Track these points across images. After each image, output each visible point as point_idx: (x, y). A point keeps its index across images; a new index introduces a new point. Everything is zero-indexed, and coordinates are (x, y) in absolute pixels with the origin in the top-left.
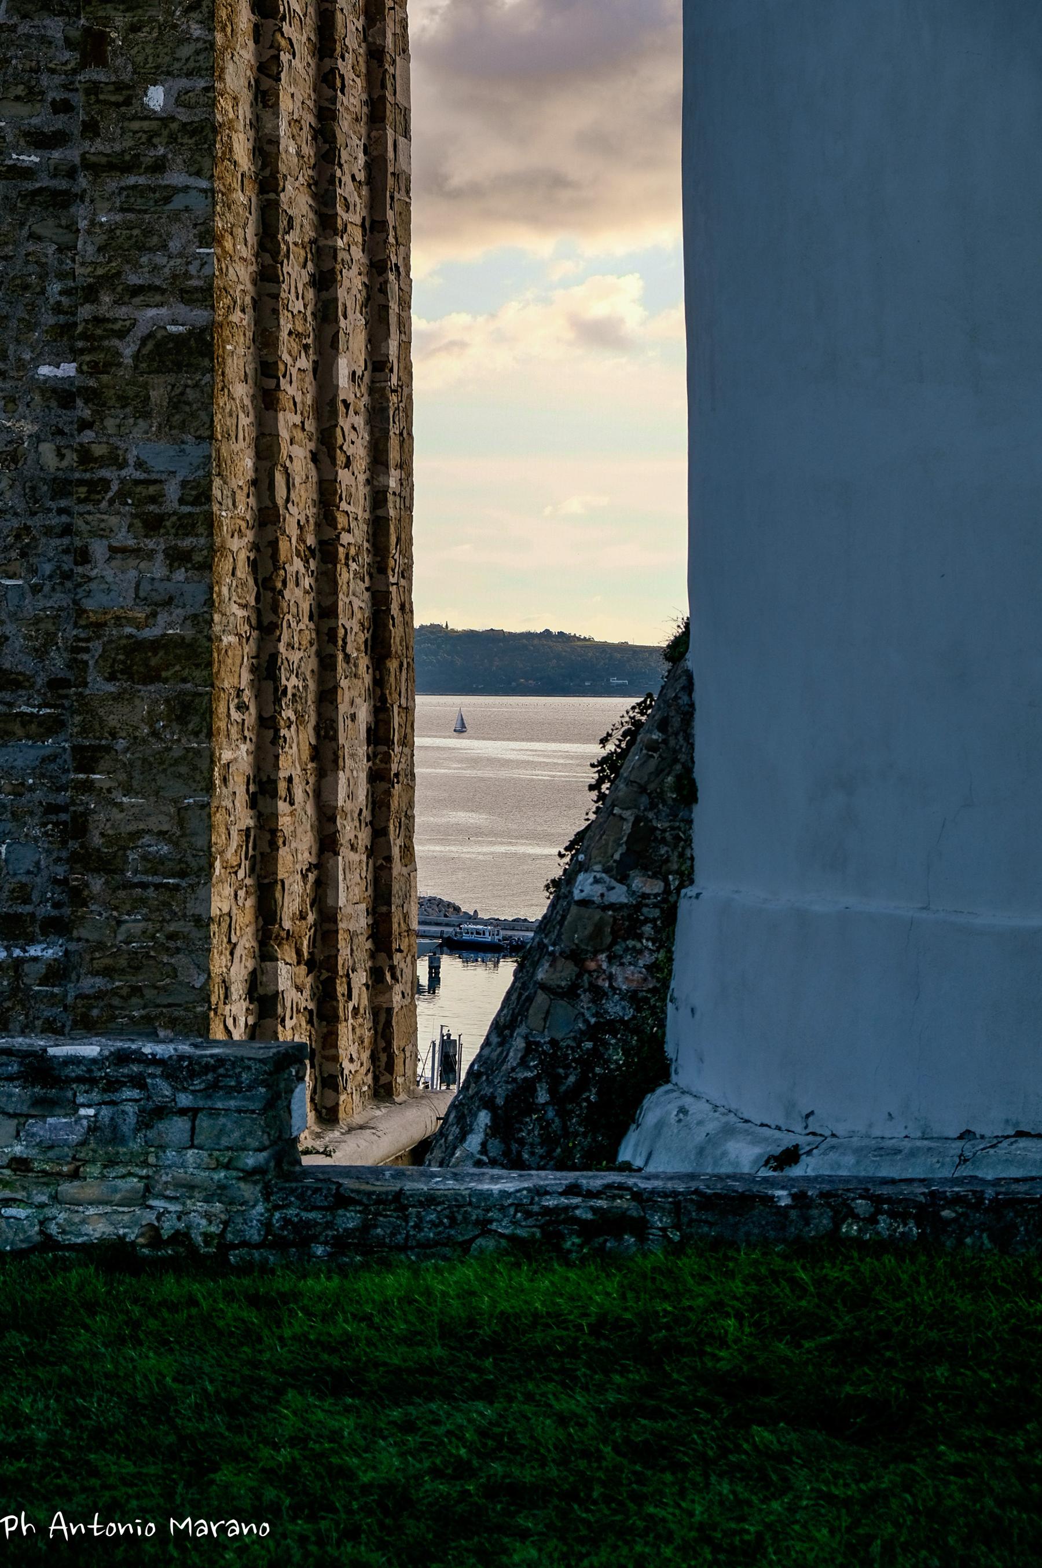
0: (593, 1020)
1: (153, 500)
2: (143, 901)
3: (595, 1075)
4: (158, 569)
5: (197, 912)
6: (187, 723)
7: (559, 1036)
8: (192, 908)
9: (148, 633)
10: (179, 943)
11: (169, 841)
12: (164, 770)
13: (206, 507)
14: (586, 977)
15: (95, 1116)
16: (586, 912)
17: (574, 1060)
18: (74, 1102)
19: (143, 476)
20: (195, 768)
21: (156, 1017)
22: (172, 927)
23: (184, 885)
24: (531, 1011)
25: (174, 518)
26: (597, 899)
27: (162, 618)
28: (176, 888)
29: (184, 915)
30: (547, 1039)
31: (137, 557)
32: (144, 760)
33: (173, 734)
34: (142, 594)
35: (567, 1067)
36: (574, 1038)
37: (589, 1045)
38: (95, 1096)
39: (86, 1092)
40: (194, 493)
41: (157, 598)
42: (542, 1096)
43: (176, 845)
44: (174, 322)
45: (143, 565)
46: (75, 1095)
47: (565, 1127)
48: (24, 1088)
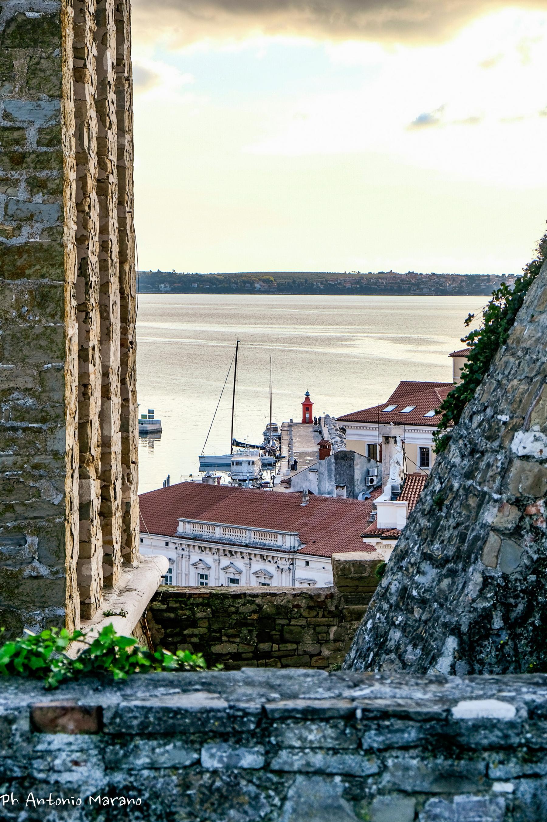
0: (535, 557)
1: (17, 142)
2: (14, 441)
3: (538, 603)
4: (22, 193)
5: (55, 448)
6: (45, 308)
7: (509, 571)
8: (52, 445)
9: (15, 241)
10: (42, 472)
11: (33, 396)
12: (29, 344)
13: (57, 148)
14: (527, 519)
15: (514, 793)
16: (528, 465)
17: (522, 591)
18: (487, 775)
19: (10, 124)
20: (52, 342)
21: (25, 527)
22: (36, 460)
23: (45, 428)
24: (485, 550)
25: (33, 156)
26: (537, 455)
27: (26, 230)
28: (39, 430)
29: (46, 451)
30: (500, 574)
31: (6, 185)
32: (13, 336)
33: (35, 316)
34: (10, 212)
35: (516, 597)
36: (521, 573)
37: (533, 578)
38: (512, 767)
39: (501, 762)
40: (48, 137)
41: (22, 215)
42: (497, 623)
43: (38, 398)
44: (31, 10)
45: (10, 191)
46: (487, 767)
47: (516, 649)
48: (423, 759)
